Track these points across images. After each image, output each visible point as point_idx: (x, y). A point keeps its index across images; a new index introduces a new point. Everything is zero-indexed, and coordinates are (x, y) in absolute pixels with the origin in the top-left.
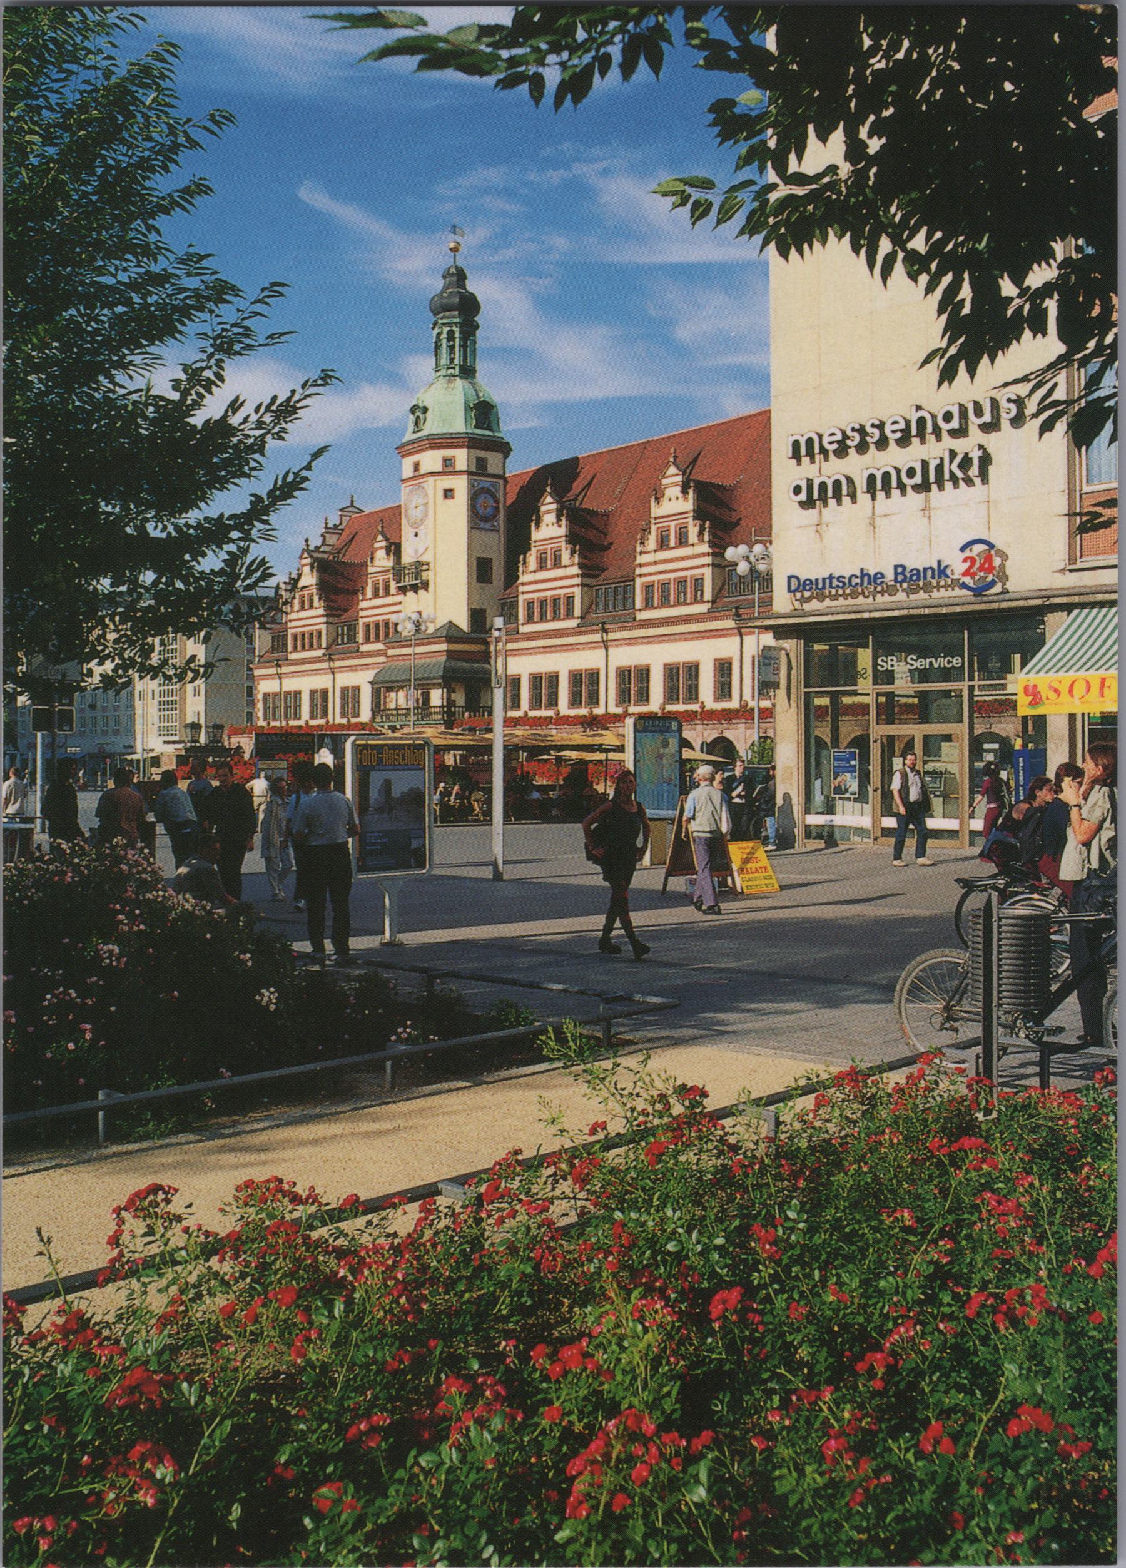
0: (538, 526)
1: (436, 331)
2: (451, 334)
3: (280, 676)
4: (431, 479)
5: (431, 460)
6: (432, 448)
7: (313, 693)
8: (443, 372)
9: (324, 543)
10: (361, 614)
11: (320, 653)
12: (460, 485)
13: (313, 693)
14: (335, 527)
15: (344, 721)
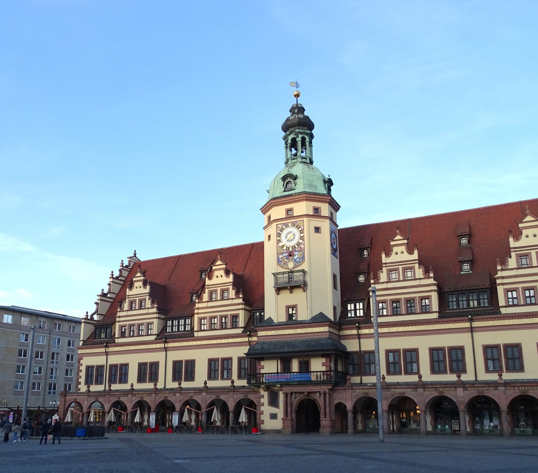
0: (388, 255)
1: (290, 138)
2: (303, 139)
3: (107, 354)
4: (305, 219)
5: (302, 208)
6: (307, 200)
7: (142, 366)
8: (299, 160)
9: (121, 275)
10: (196, 311)
11: (153, 338)
12: (325, 226)
13: (142, 366)
14: (127, 266)
15: (175, 385)
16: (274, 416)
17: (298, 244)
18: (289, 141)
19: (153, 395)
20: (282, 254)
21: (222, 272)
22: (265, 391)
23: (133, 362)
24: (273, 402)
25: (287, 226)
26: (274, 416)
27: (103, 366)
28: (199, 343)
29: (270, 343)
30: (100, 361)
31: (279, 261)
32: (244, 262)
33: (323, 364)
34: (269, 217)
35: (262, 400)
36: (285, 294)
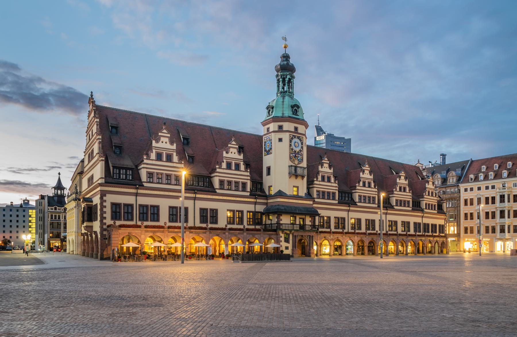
3: (136, 195)
16: (287, 248)
17: (300, 151)
18: (287, 79)
19: (208, 233)
20: (292, 154)
21: (235, 151)
22: (282, 233)
23: (165, 205)
24: (287, 240)
25: (295, 137)
26: (287, 248)
27: (132, 206)
28: (221, 198)
29: (287, 207)
30: (130, 200)
31: (290, 158)
32: (253, 150)
33: (310, 221)
34: (280, 127)
35: (281, 239)
36: (293, 178)
